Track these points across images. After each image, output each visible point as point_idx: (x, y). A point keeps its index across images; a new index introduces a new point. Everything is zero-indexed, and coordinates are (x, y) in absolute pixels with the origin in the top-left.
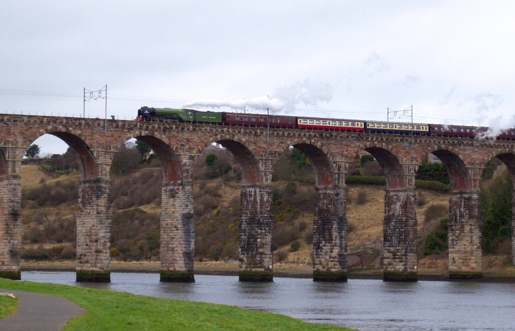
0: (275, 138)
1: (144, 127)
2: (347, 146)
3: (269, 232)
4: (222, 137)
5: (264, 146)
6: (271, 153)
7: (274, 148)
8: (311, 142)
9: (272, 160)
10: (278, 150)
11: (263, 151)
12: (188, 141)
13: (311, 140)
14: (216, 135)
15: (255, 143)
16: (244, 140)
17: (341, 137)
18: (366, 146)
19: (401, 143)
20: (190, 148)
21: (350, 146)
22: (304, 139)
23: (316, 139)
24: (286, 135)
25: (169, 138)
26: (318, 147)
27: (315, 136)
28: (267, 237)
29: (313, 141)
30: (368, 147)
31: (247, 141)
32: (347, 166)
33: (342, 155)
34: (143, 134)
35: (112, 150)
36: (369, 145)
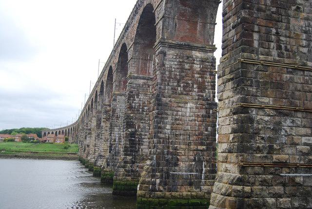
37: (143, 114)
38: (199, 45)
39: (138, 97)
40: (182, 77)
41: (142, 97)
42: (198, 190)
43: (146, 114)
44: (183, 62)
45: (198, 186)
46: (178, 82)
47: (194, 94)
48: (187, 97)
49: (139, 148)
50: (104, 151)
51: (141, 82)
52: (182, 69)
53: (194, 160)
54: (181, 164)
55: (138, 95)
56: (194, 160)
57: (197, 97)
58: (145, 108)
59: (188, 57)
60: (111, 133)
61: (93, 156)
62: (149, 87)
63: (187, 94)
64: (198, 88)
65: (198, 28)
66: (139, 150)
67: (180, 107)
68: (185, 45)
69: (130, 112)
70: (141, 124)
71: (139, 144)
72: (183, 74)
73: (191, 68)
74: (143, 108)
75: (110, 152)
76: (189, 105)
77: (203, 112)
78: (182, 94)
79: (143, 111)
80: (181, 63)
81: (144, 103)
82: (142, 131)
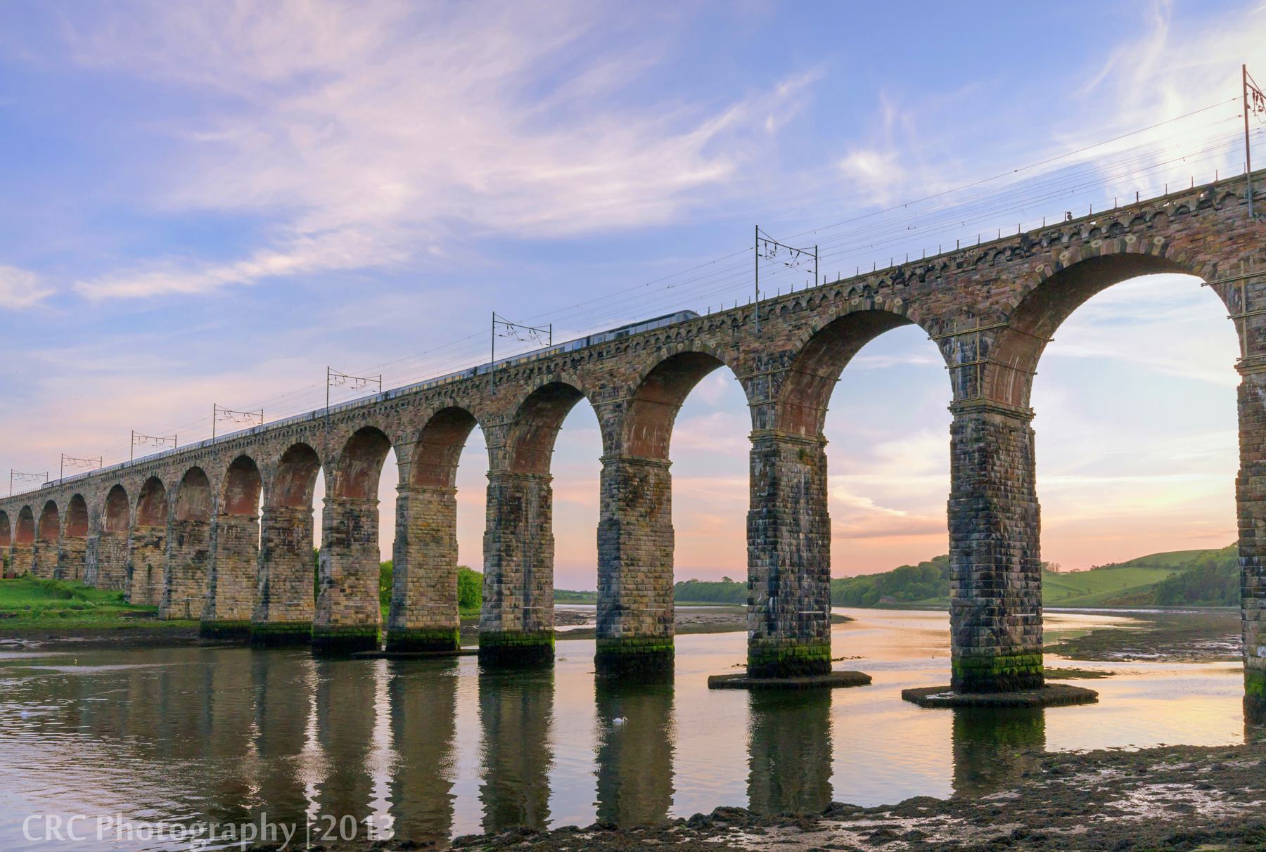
0: (780, 320)
1: (544, 368)
2: (986, 283)
3: (764, 550)
4: (669, 350)
5: (756, 345)
6: (773, 358)
7: (780, 345)
8: (873, 303)
9: (774, 375)
10: (788, 347)
11: (754, 359)
12: (612, 375)
13: (872, 297)
14: (659, 349)
15: (736, 346)
16: (712, 343)
17: (959, 266)
18: (1058, 264)
19: (1209, 212)
20: (614, 388)
21: (996, 280)
22: (855, 301)
23: (885, 290)
24: (804, 304)
25: (582, 378)
26: (895, 311)
27: (882, 284)
28: (759, 562)
29: (878, 299)
30: (1065, 265)
31: (718, 345)
32: (989, 341)
33: (970, 312)
34: (545, 383)
35: (506, 421)
36: (1071, 259)
50: (627, 595)
51: (998, 419)
58: (1009, 483)
60: (775, 543)
61: (496, 611)
69: (990, 493)
71: (1007, 569)
74: (1005, 485)
75: (773, 593)
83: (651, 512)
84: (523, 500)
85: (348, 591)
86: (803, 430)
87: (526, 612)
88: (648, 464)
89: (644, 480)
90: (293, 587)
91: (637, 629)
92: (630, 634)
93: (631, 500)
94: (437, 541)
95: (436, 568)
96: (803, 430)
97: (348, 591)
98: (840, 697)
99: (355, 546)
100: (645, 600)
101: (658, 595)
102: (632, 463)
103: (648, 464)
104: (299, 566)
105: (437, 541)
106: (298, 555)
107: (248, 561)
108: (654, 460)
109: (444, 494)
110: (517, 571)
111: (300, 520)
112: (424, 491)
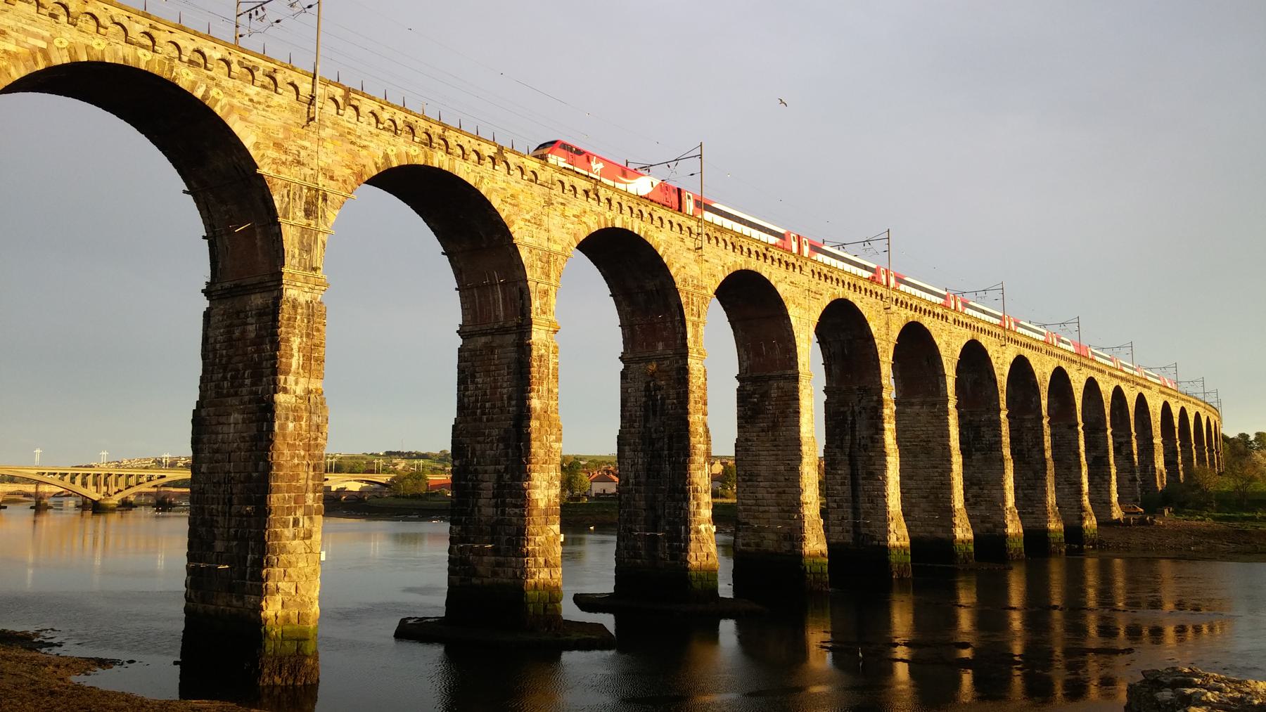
37: (481, 420)
38: (254, 280)
39: (473, 382)
40: (230, 357)
41: (480, 380)
42: (240, 603)
43: (488, 420)
44: (231, 325)
45: (241, 598)
46: (225, 370)
47: (244, 390)
48: (235, 401)
49: (475, 505)
50: (745, 510)
52: (230, 342)
53: (235, 537)
54: (219, 546)
55: (473, 376)
56: (235, 537)
57: (246, 398)
59: (238, 313)
62: (492, 352)
63: (236, 394)
64: (252, 376)
65: (259, 243)
66: (473, 510)
67: (219, 423)
68: (236, 286)
70: (478, 447)
72: (231, 352)
73: (243, 336)
74: (483, 407)
76: (232, 420)
77: (254, 431)
78: (228, 395)
79: (483, 413)
80: (229, 329)
81: (485, 394)
82: (478, 463)
83: (774, 426)
84: (848, 413)
85: (972, 500)
86: (660, 346)
87: (856, 526)
88: (771, 378)
89: (765, 396)
90: (1025, 495)
91: (758, 545)
92: (752, 549)
93: (750, 417)
94: (928, 451)
95: (927, 479)
96: (660, 346)
97: (972, 500)
98: (435, 604)
99: (977, 456)
100: (766, 516)
101: (783, 511)
102: (754, 380)
103: (771, 378)
104: (1030, 474)
105: (928, 451)
106: (1028, 463)
107: (1069, 469)
108: (779, 373)
109: (934, 405)
110: (843, 484)
111: (1029, 429)
112: (912, 404)
